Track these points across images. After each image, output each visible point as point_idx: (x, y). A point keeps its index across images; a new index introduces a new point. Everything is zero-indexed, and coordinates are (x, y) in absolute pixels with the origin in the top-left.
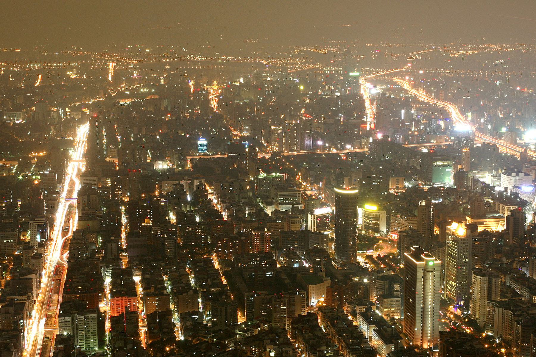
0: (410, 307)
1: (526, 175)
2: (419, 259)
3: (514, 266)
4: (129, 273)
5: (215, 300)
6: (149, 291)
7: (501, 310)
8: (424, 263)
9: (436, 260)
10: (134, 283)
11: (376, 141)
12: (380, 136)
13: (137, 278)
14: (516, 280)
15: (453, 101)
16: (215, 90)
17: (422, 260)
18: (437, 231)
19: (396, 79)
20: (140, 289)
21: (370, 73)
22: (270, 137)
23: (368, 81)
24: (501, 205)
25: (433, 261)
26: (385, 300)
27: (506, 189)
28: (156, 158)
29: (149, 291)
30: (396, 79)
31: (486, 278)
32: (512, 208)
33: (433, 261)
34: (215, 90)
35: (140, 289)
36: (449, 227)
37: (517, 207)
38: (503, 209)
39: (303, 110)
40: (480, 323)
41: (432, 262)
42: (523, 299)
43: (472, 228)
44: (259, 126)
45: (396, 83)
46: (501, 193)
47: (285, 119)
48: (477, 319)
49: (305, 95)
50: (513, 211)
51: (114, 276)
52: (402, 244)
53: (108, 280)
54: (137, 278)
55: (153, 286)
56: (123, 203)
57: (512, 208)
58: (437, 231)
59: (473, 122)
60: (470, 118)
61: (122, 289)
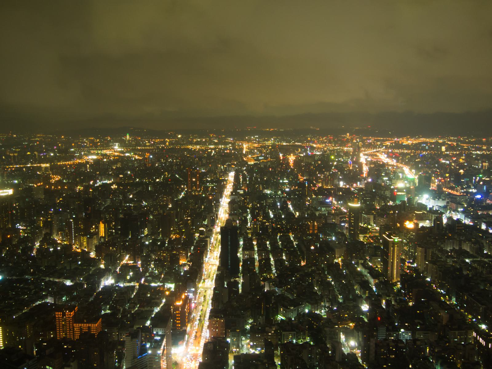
0: (385, 262)
1: (443, 200)
2: (391, 238)
3: (438, 244)
4: (251, 240)
5: (292, 253)
6: (260, 249)
7: (431, 264)
8: (392, 240)
9: (398, 239)
10: (253, 244)
11: (368, 183)
12: (370, 180)
13: (255, 243)
14: (439, 251)
15: (407, 164)
16: (292, 158)
17: (391, 238)
18: (398, 225)
19: (378, 154)
20: (256, 249)
21: (365, 151)
22: (317, 179)
23: (365, 155)
24: (431, 214)
25: (397, 239)
26: (373, 258)
27: (433, 206)
28: (264, 188)
29: (260, 249)
30: (378, 154)
31: (424, 249)
32: (436, 215)
33: (397, 239)
34: (292, 158)
35: (256, 249)
36: (405, 223)
37: (438, 215)
38: (432, 216)
39: (333, 168)
40: (421, 270)
41: (397, 239)
42: (442, 260)
43: (417, 225)
44: (311, 174)
45: (378, 156)
46: (430, 208)
47: (325, 171)
48: (419, 269)
49: (334, 161)
50: (436, 217)
51: (244, 241)
52: (381, 232)
53: (241, 243)
54: (255, 243)
55: (262, 246)
56: (248, 208)
57: (436, 215)
58: (398, 225)
59: (416, 174)
60: (414, 173)
61: (248, 247)
